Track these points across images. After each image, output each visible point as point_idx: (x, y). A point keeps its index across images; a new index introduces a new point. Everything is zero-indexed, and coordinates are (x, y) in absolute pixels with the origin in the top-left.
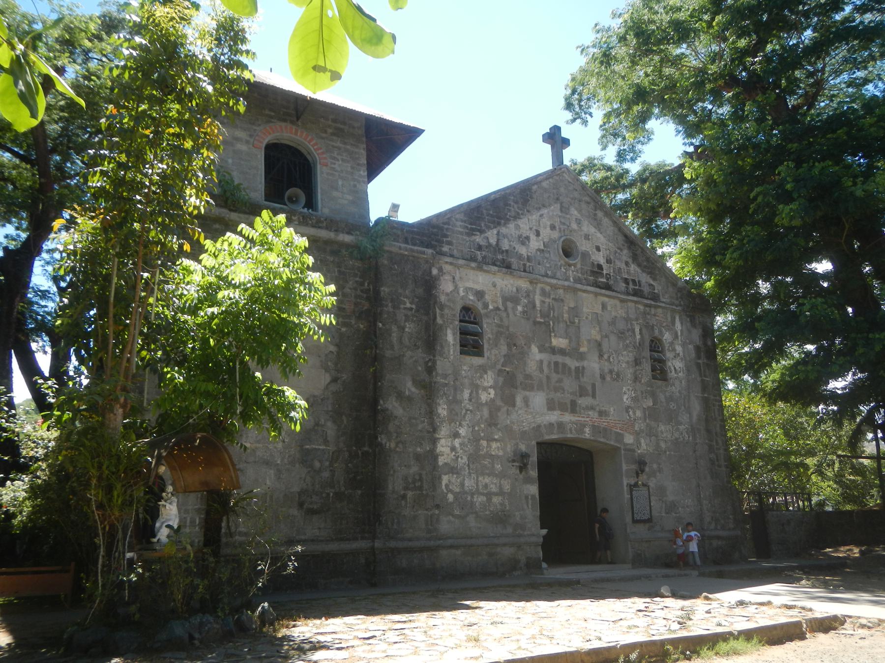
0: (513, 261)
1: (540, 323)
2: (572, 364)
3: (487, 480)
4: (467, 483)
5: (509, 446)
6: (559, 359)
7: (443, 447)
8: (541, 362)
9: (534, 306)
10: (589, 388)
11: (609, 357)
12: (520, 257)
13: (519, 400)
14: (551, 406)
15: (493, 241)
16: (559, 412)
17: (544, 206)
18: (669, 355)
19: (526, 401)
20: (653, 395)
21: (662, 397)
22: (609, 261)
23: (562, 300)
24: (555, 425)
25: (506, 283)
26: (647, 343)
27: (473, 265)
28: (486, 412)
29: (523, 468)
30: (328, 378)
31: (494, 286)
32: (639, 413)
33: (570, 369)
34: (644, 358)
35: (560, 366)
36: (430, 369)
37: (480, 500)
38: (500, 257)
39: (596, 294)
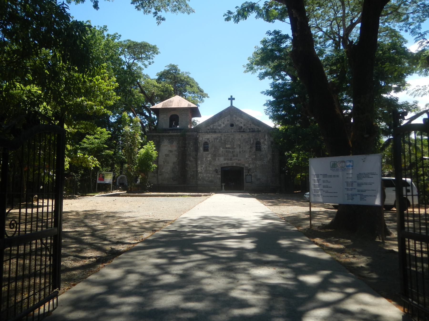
0: (217, 131)
2: (231, 150)
3: (208, 175)
4: (204, 175)
6: (228, 150)
7: (199, 169)
8: (223, 151)
9: (222, 139)
10: (236, 155)
12: (219, 129)
13: (217, 159)
14: (225, 160)
15: (212, 127)
17: (226, 116)
18: (262, 145)
19: (219, 159)
20: (256, 155)
21: (259, 155)
22: (244, 125)
23: (230, 137)
25: (215, 136)
27: (206, 133)
28: (209, 162)
29: (217, 172)
30: (177, 159)
31: (212, 137)
32: (250, 159)
33: (230, 152)
36: (196, 155)
37: (207, 178)
38: (213, 130)
39: (240, 134)
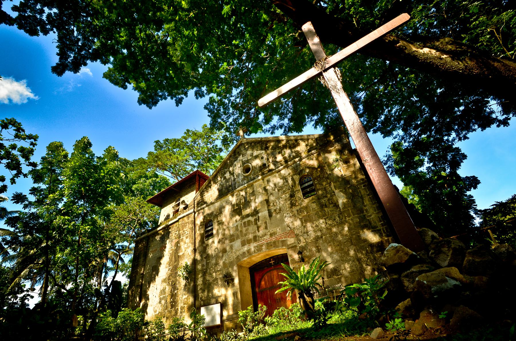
1: (237, 209)
5: (224, 271)
11: (274, 204)
14: (243, 244)
16: (248, 245)
24: (246, 252)
26: (297, 182)
34: (296, 191)
35: (246, 223)
